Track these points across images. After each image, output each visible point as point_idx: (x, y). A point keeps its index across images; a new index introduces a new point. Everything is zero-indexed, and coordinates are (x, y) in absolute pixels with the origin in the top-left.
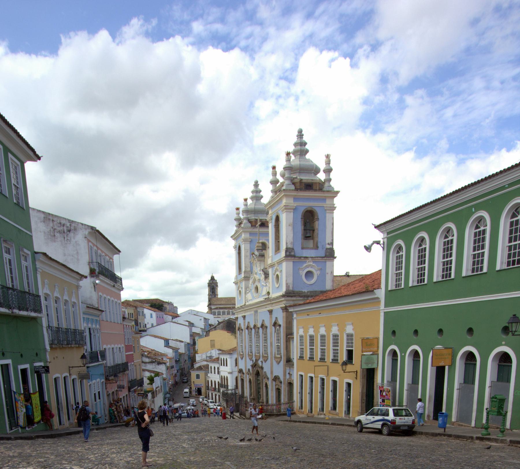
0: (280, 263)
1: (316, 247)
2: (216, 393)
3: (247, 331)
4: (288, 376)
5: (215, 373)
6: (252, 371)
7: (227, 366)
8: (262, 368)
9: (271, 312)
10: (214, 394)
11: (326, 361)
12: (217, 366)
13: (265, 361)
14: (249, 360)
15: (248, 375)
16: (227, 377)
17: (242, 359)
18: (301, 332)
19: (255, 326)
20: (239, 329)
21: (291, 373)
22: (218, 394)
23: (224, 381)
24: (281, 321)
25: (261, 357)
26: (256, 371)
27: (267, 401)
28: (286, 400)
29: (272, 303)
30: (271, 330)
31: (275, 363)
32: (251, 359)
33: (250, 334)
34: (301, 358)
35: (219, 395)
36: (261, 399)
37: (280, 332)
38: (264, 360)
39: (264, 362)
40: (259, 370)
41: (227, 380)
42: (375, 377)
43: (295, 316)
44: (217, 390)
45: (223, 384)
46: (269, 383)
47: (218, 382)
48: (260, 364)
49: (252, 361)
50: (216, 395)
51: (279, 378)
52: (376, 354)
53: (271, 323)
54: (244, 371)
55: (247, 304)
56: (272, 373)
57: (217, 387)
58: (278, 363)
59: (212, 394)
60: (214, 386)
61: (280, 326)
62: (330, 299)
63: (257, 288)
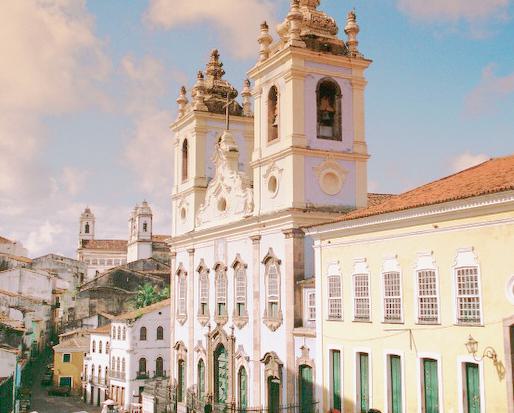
0: (187, 193)
1: (337, 137)
3: (197, 274)
4: (299, 353)
5: (100, 351)
6: (209, 345)
7: (124, 338)
8: (234, 340)
9: (257, 239)
11: (439, 322)
12: (105, 339)
13: (241, 327)
14: (200, 325)
15: (195, 353)
16: (124, 359)
18: (334, 271)
19: (217, 266)
20: (179, 273)
21: (308, 346)
23: (118, 367)
25: (230, 319)
26: (216, 344)
27: (243, 400)
28: (296, 400)
29: (196, 240)
30: (256, 271)
31: (265, 330)
32: (203, 324)
33: (204, 282)
37: (279, 272)
38: (239, 325)
39: (236, 328)
40: (227, 345)
41: (124, 363)
43: (317, 243)
45: (116, 370)
46: (250, 368)
48: (229, 333)
49: (206, 328)
51: (276, 357)
53: (255, 260)
54: (187, 346)
55: (197, 230)
56: (257, 346)
57: (103, 375)
60: (96, 373)
61: (279, 262)
62: (417, 206)
63: (223, 205)
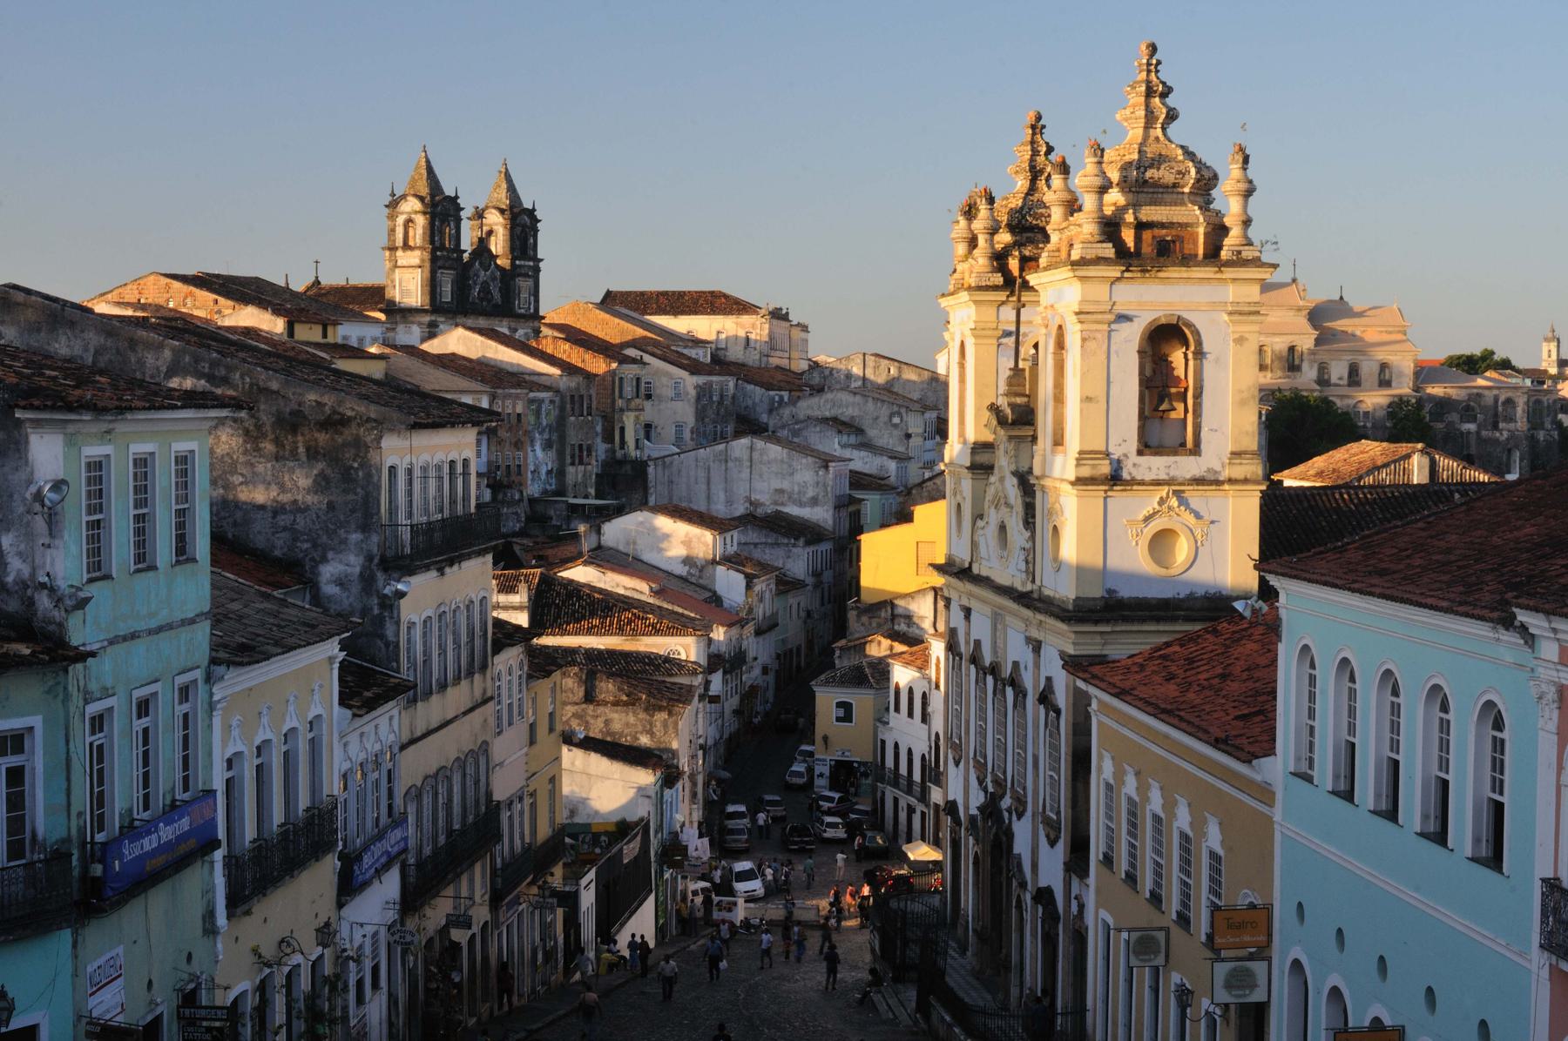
2: (913, 801)
4: (1074, 904)
5: (911, 715)
10: (902, 804)
17: (957, 764)
22: (920, 808)
24: (1061, 698)
34: (1108, 860)
35: (923, 814)
36: (1004, 951)
42: (1266, 1029)
44: (917, 789)
47: (923, 756)
50: (911, 810)
52: (1263, 959)
53: (1036, 686)
57: (917, 777)
58: (1052, 843)
59: (896, 800)
60: (903, 770)
61: (1058, 712)
